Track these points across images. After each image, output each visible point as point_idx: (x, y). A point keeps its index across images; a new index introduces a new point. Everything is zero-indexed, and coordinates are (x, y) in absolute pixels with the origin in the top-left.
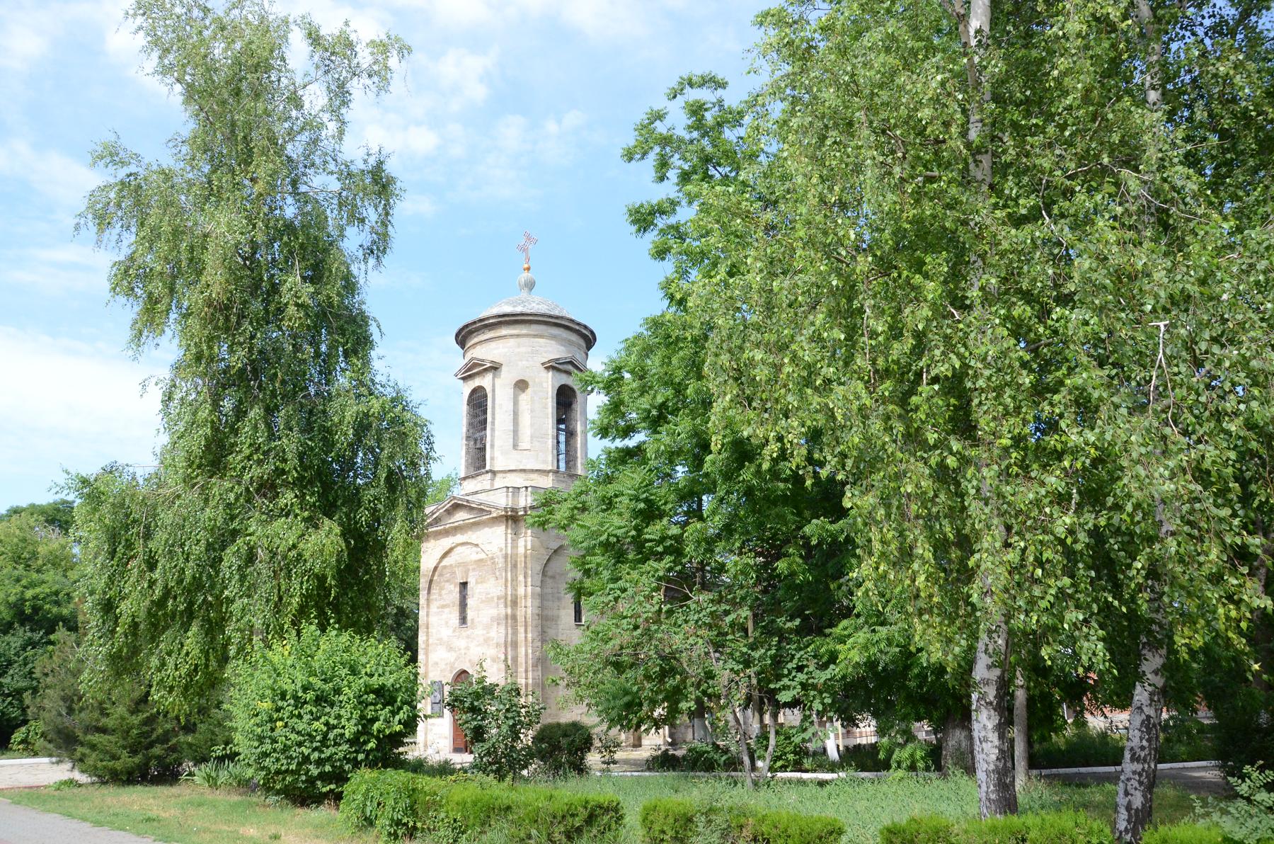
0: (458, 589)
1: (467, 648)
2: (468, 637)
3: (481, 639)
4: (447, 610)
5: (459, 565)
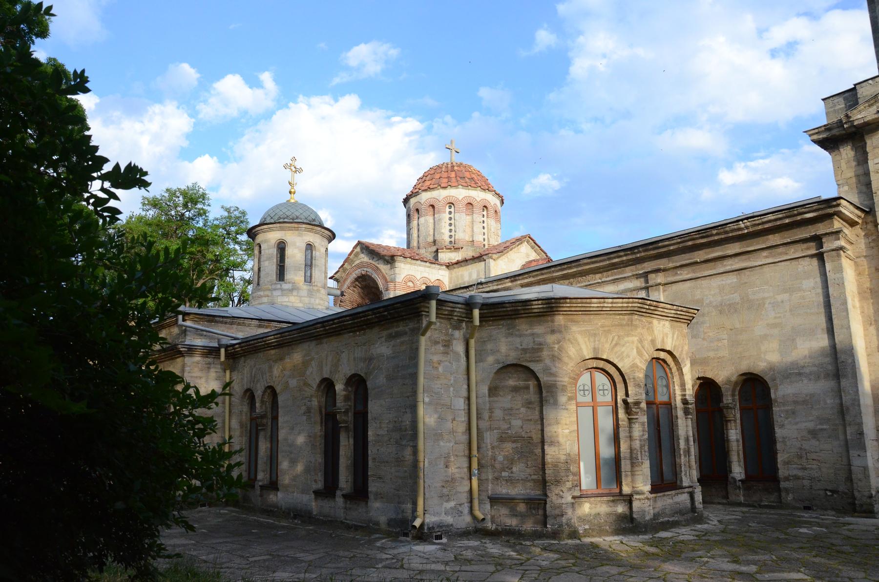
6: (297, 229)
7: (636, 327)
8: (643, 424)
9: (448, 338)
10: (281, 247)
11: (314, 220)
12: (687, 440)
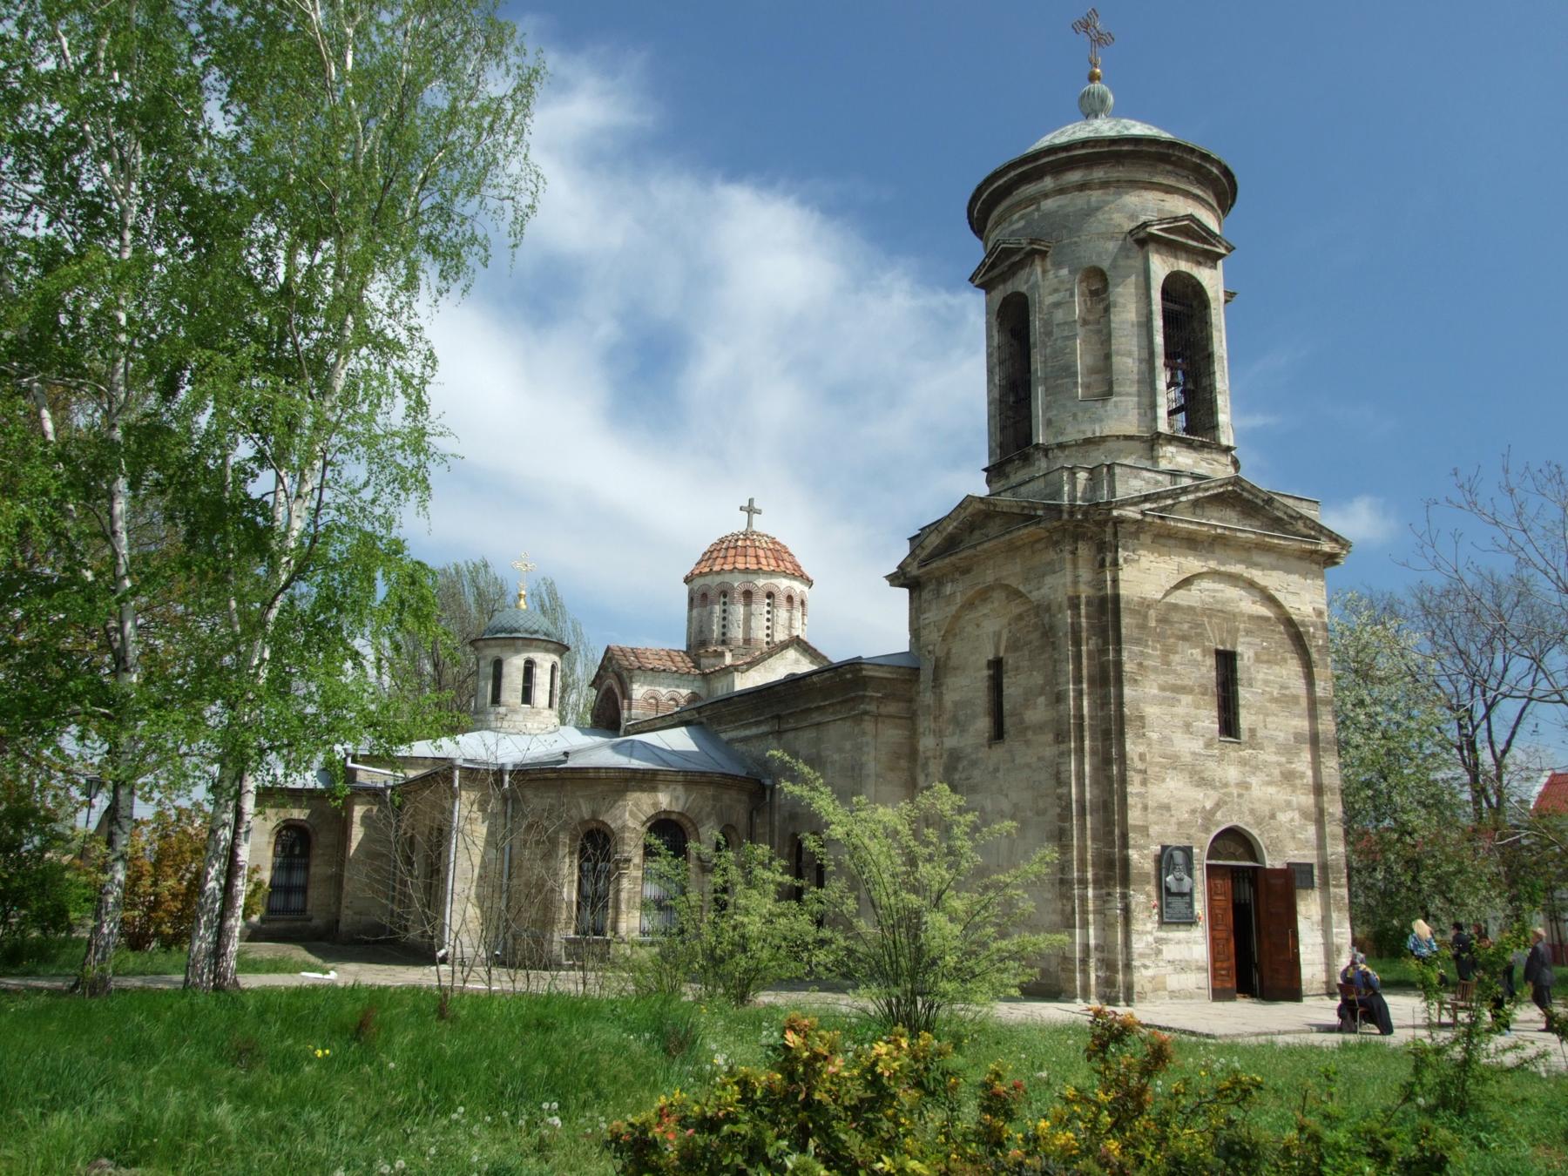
0: (1211, 661)
1: (1245, 786)
2: (1243, 762)
3: (1276, 772)
4: (1186, 699)
5: (1210, 612)
10: (498, 665)
11: (536, 632)
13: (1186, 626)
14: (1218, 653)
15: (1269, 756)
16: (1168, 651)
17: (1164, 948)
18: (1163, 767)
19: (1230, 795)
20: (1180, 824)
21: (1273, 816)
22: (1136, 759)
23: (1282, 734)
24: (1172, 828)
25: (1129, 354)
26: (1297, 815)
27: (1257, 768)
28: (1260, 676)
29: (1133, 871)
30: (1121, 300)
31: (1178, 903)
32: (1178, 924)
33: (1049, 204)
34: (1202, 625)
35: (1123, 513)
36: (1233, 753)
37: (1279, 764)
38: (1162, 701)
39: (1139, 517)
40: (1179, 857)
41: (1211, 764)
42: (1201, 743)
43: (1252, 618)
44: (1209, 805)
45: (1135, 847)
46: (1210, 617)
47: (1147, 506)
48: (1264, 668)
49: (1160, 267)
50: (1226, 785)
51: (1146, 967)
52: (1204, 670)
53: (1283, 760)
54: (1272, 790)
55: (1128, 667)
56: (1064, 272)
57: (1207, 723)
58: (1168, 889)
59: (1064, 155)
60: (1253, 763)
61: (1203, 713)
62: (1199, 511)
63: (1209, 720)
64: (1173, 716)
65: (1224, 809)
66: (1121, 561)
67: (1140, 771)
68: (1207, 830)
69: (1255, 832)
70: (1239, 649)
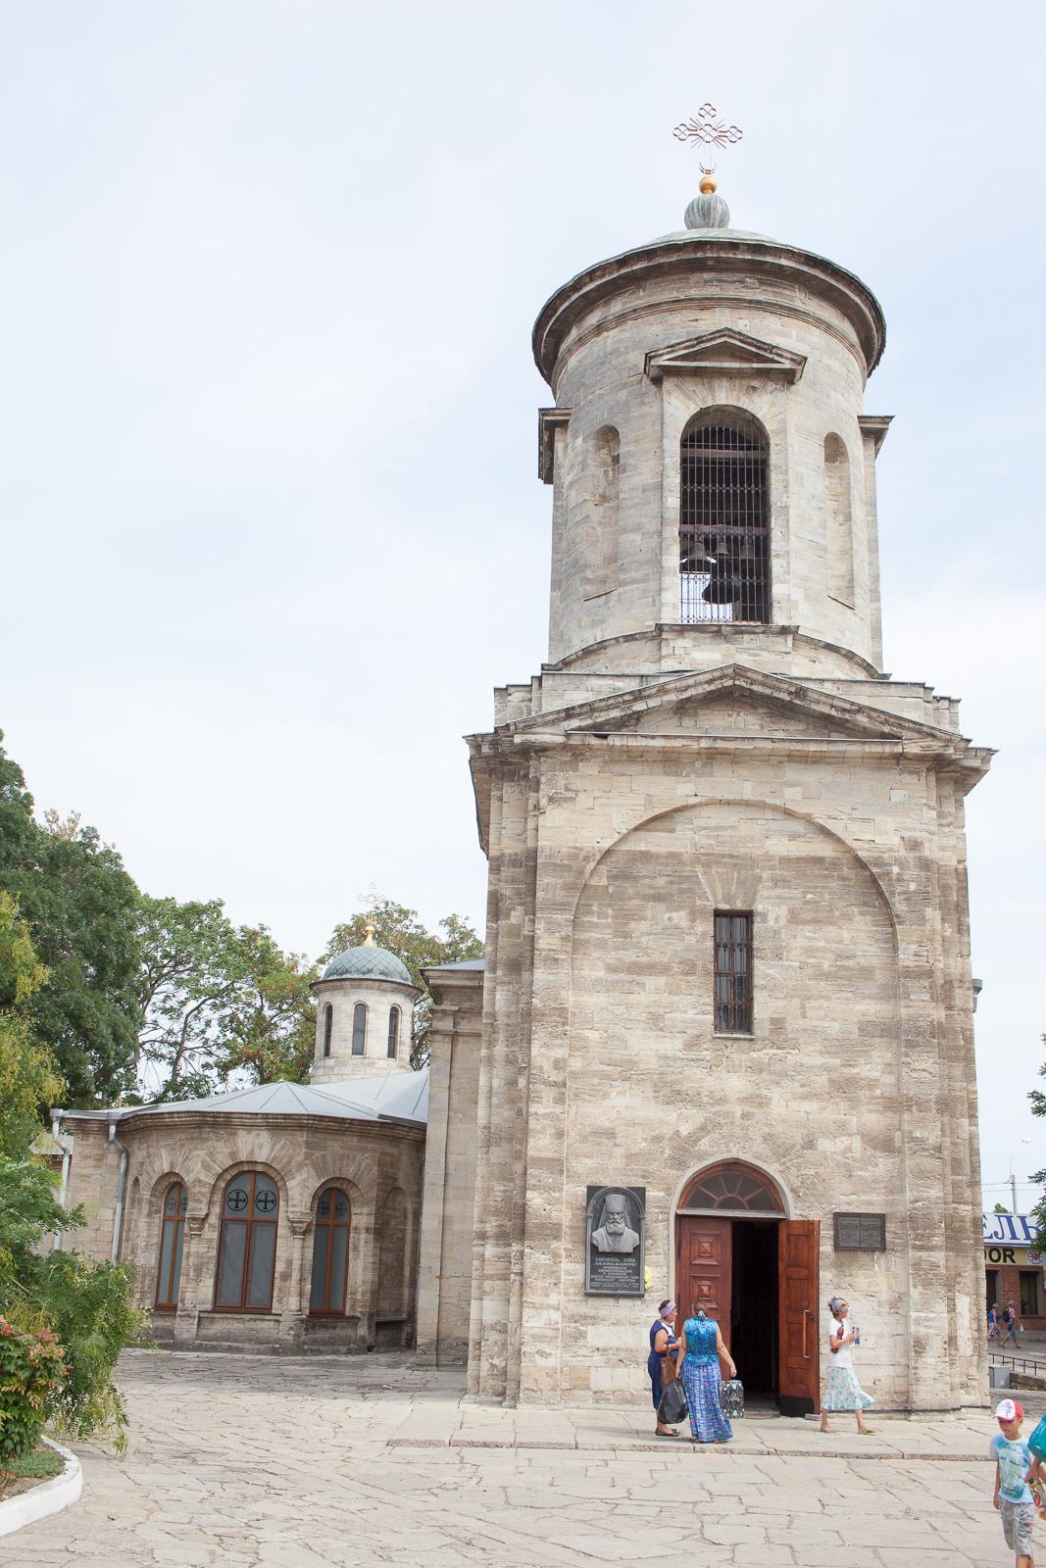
0: (706, 927)
1: (761, 1102)
2: (757, 1068)
3: (822, 1080)
5: (709, 860)
6: (342, 988)
7: (206, 1140)
8: (210, 1241)
9: (101, 1152)
11: (370, 971)
12: (289, 1263)
13: (661, 881)
14: (718, 914)
15: (810, 1056)
16: (625, 917)
17: (590, 1329)
18: (609, 1077)
19: (727, 1114)
20: (630, 1157)
21: (810, 1144)
22: (547, 1066)
23: (836, 1025)
24: (618, 1162)
25: (638, 528)
26: (857, 1143)
27: (784, 1075)
28: (800, 942)
29: (531, 1221)
30: (632, 461)
31: (615, 1270)
32: (617, 1297)
33: (573, 361)
34: (693, 878)
35: (532, 738)
36: (738, 1053)
37: (828, 1069)
38: (612, 987)
39: (560, 739)
40: (617, 1203)
41: (696, 1072)
42: (678, 1042)
43: (785, 861)
44: (685, 1130)
45: (535, 1188)
46: (707, 865)
47: (575, 723)
48: (807, 930)
49: (680, 407)
50: (722, 1101)
51: (541, 1353)
52: (691, 940)
53: (837, 1062)
54: (806, 1106)
55: (544, 942)
56: (580, 440)
57: (691, 1014)
58: (594, 1248)
59: (576, 295)
60: (778, 1067)
61: (682, 1000)
62: (687, 722)
63: (696, 1007)
64: (628, 1006)
65: (715, 1135)
66: (544, 802)
67: (555, 1084)
68: (680, 1164)
69: (772, 1169)
70: (759, 907)
